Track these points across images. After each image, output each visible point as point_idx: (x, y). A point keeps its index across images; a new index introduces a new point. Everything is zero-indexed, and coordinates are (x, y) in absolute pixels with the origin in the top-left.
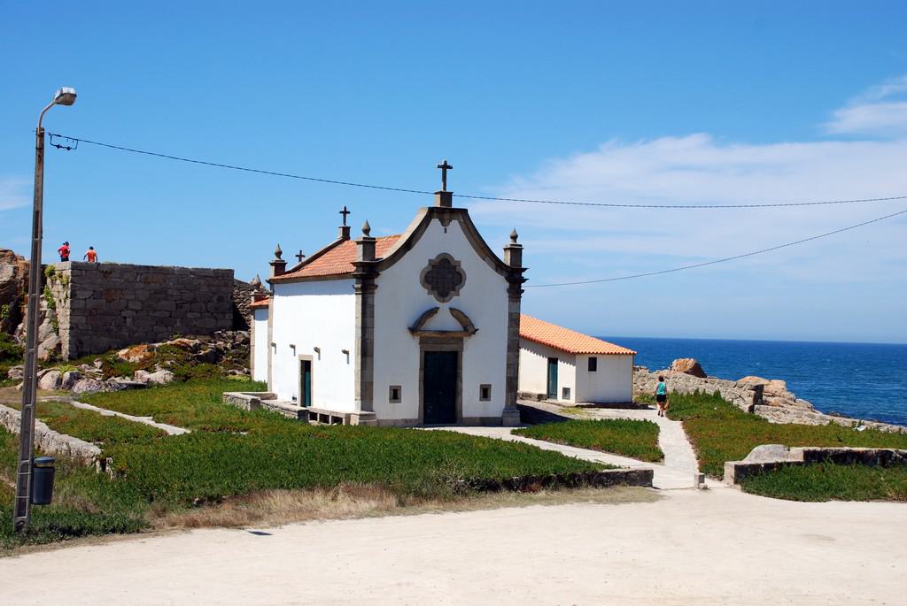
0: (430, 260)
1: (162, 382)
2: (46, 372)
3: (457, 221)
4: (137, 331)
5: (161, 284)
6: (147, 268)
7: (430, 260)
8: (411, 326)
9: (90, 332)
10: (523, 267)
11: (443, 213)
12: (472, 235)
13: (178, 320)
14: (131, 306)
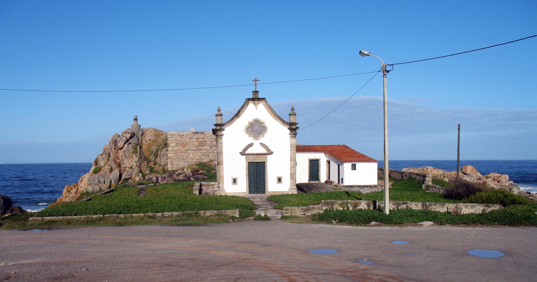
0: (249, 122)
3: (262, 104)
4: (194, 159)
7: (249, 122)
8: (241, 151)
14: (191, 149)
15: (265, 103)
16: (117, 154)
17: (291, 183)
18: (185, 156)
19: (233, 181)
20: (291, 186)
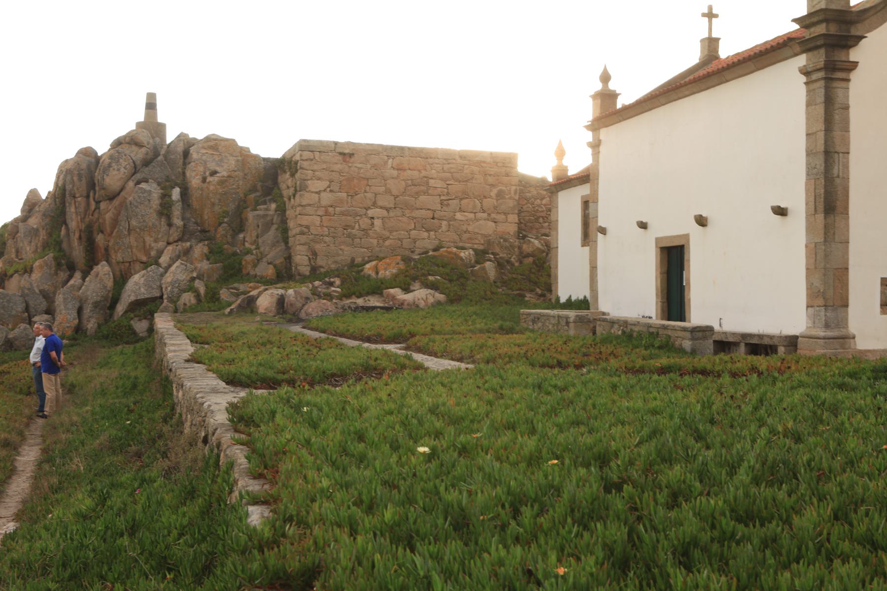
1: (422, 304)
2: (266, 289)
4: (388, 238)
5: (419, 171)
6: (402, 149)
9: (327, 239)
13: (444, 223)
14: (380, 203)
16: (96, 215)
18: (357, 226)
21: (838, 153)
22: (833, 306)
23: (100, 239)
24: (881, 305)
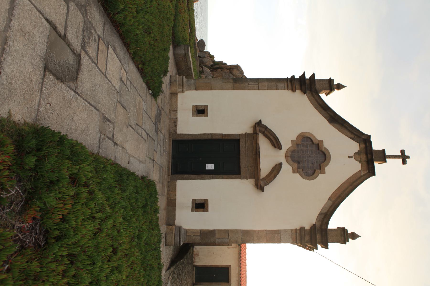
0: (322, 141)
3: (360, 168)
7: (322, 141)
10: (329, 244)
11: (367, 154)
12: (351, 185)
15: (364, 175)
17: (192, 231)
19: (202, 108)
20: (186, 231)
21: (258, 84)
22: (196, 83)
23: (220, 70)
24: (196, 106)
